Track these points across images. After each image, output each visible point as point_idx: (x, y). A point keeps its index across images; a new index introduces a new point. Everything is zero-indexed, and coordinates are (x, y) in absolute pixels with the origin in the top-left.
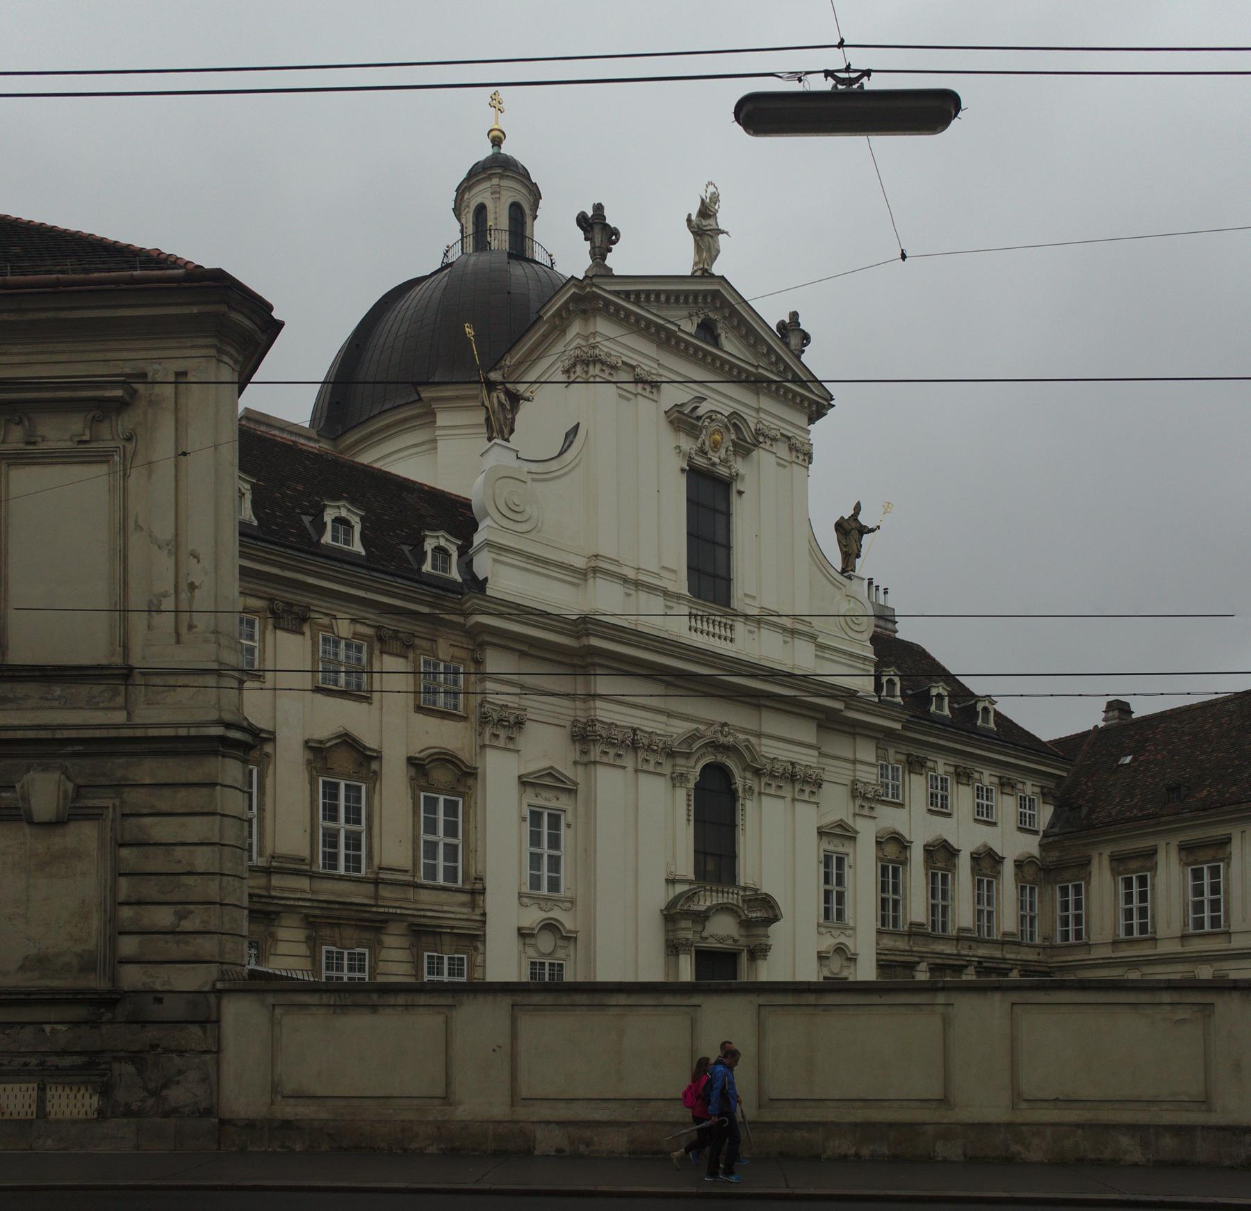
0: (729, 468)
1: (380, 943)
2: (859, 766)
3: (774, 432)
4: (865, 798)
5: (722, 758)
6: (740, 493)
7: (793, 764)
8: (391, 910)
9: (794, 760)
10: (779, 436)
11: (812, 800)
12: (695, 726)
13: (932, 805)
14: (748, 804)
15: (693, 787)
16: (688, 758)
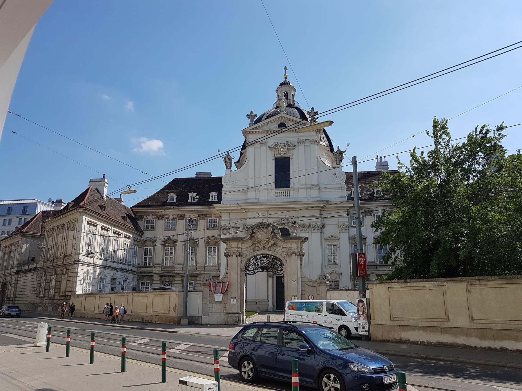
1: (196, 280)
3: (303, 140)
8: (198, 273)
10: (305, 140)
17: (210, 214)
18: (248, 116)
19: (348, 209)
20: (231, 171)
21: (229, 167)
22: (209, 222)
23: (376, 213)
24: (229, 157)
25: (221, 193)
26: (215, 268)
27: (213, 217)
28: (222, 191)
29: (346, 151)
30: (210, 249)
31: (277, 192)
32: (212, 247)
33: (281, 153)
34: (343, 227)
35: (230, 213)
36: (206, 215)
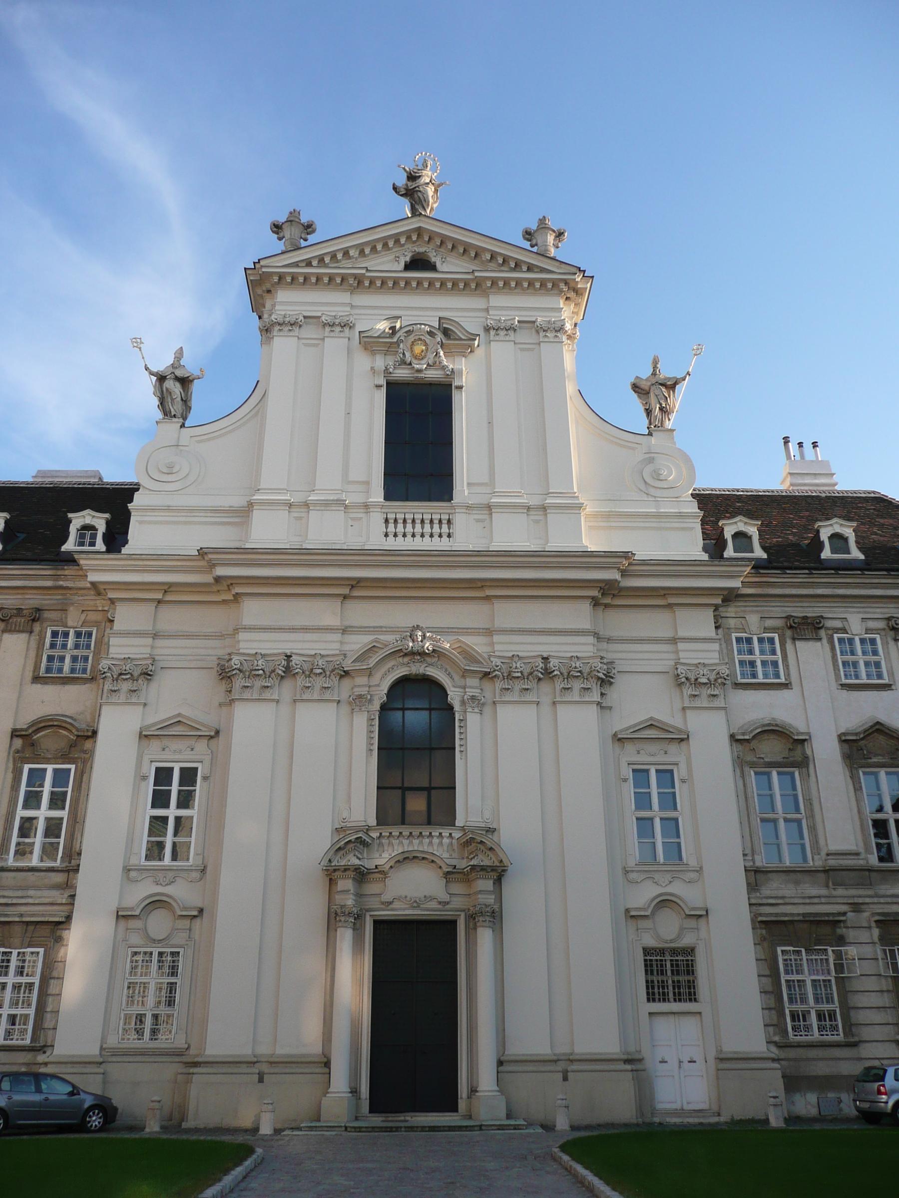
2: (681, 646)
4: (697, 683)
6: (460, 388)
7: (546, 659)
9: (545, 655)
12: (372, 637)
15: (378, 708)
16: (370, 675)
17: (59, 607)
18: (277, 228)
19: (718, 601)
21: (176, 407)
22: (53, 646)
23: (837, 630)
24: (179, 373)
25: (127, 515)
26: (53, 874)
27: (75, 624)
28: (130, 506)
30: (36, 777)
31: (391, 516)
32: (50, 768)
33: (414, 361)
34: (704, 680)
35: (161, 606)
36: (38, 610)
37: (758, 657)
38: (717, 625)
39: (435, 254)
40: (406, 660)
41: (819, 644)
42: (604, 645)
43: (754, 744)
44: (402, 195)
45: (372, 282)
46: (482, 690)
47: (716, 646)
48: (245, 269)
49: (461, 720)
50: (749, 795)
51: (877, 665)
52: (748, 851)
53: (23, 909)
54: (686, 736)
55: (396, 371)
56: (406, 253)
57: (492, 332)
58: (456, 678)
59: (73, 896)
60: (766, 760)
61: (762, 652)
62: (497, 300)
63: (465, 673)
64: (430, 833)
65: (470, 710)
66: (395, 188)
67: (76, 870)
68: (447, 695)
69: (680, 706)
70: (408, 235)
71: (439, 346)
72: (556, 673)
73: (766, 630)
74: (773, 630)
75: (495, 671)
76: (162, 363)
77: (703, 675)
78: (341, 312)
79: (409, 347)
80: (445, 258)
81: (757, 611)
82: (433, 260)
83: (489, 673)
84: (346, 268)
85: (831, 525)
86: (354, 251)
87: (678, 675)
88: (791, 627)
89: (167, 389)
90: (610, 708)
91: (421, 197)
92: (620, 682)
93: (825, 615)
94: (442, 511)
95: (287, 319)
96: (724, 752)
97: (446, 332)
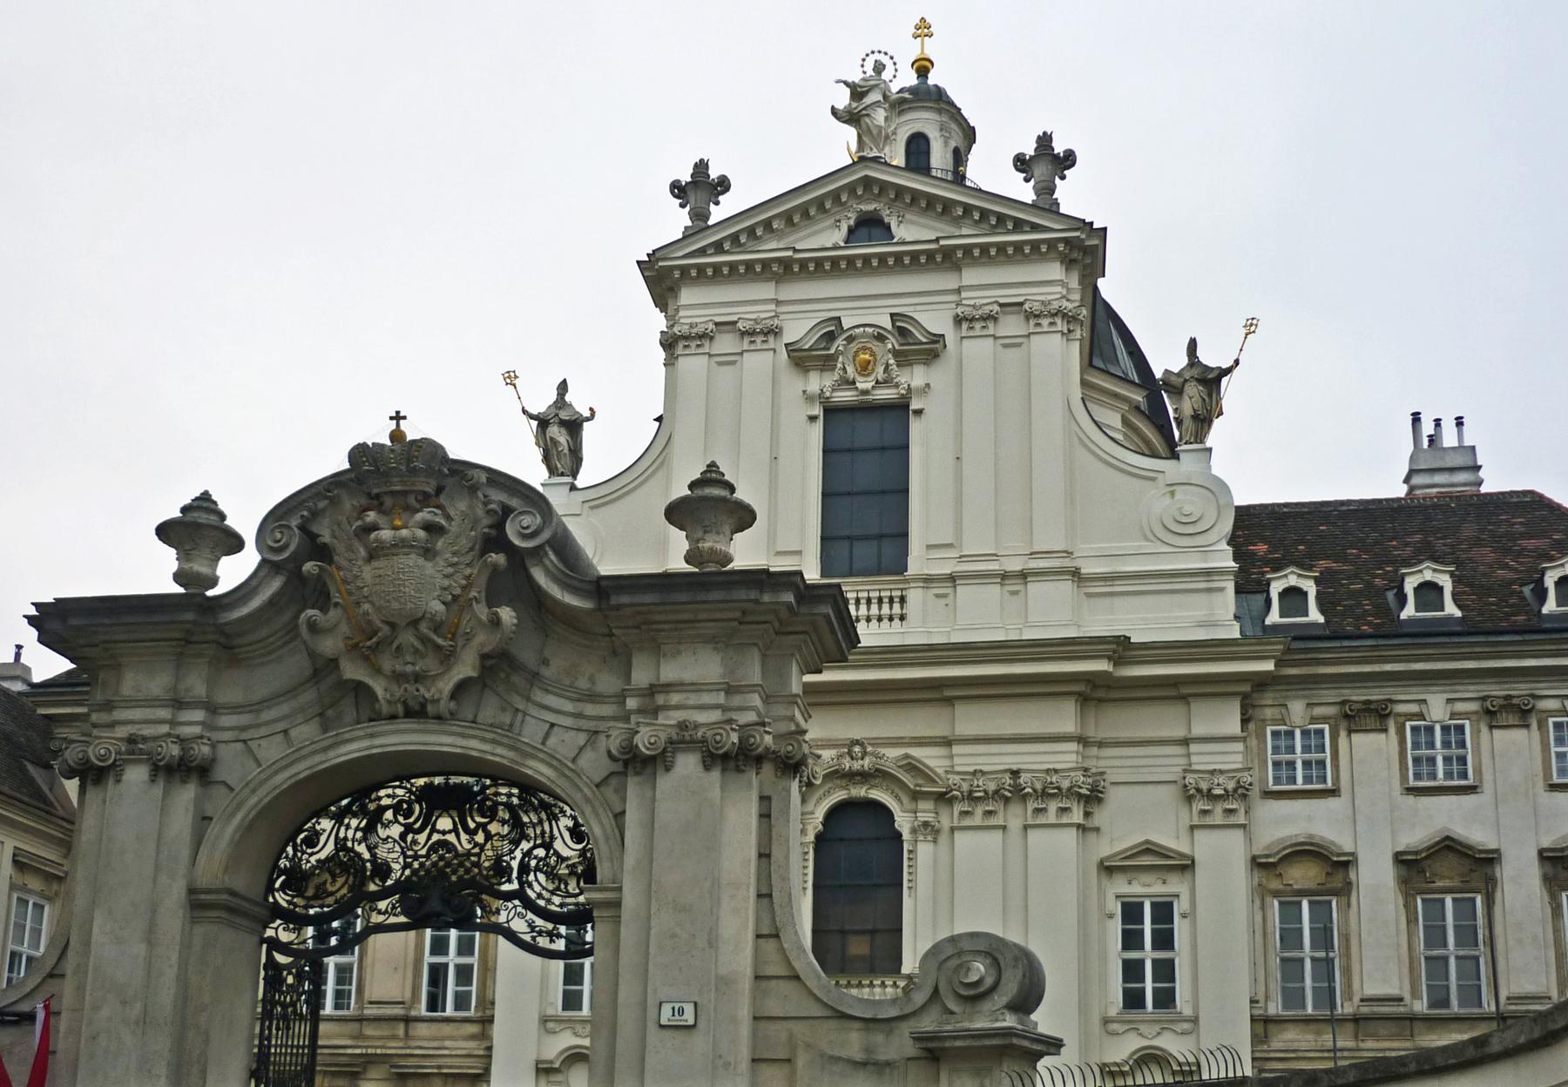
0: (897, 386)
2: (1194, 748)
3: (987, 309)
4: (1210, 796)
5: (860, 792)
7: (1015, 774)
8: (369, 1051)
9: (1015, 767)
10: (996, 308)
11: (1065, 820)
13: (1418, 776)
14: (925, 850)
18: (678, 190)
20: (573, 488)
23: (1411, 716)
24: (564, 415)
29: (1237, 362)
33: (859, 378)
37: (1299, 757)
38: (1245, 717)
39: (888, 212)
40: (844, 782)
41: (1383, 736)
42: (1094, 751)
43: (1280, 870)
44: (844, 122)
45: (803, 264)
46: (937, 813)
47: (1239, 747)
48: (638, 262)
49: (910, 852)
50: (1270, 930)
51: (1462, 760)
52: (1261, 997)
53: (441, 1061)
54: (1190, 862)
55: (835, 394)
56: (849, 215)
57: (965, 326)
58: (905, 799)
59: (490, 1048)
60: (1295, 887)
61: (1306, 749)
62: (971, 276)
63: (916, 796)
64: (871, 982)
65: (921, 838)
66: (834, 112)
67: (491, 1020)
68: (894, 821)
69: (1188, 823)
70: (851, 188)
71: (890, 356)
72: (1026, 790)
73: (1314, 720)
74: (1324, 719)
75: (952, 790)
76: (542, 402)
77: (1218, 785)
78: (764, 312)
79: (851, 359)
80: (903, 216)
81: (1304, 697)
82: (886, 220)
83: (946, 793)
84: (771, 249)
85: (1421, 571)
86: (778, 221)
87: (1185, 786)
88: (1346, 716)
89: (551, 438)
90: (1097, 830)
91: (870, 124)
92: (1116, 798)
93: (1394, 697)
94: (892, 586)
95: (695, 331)
96: (1240, 879)
97: (902, 332)
